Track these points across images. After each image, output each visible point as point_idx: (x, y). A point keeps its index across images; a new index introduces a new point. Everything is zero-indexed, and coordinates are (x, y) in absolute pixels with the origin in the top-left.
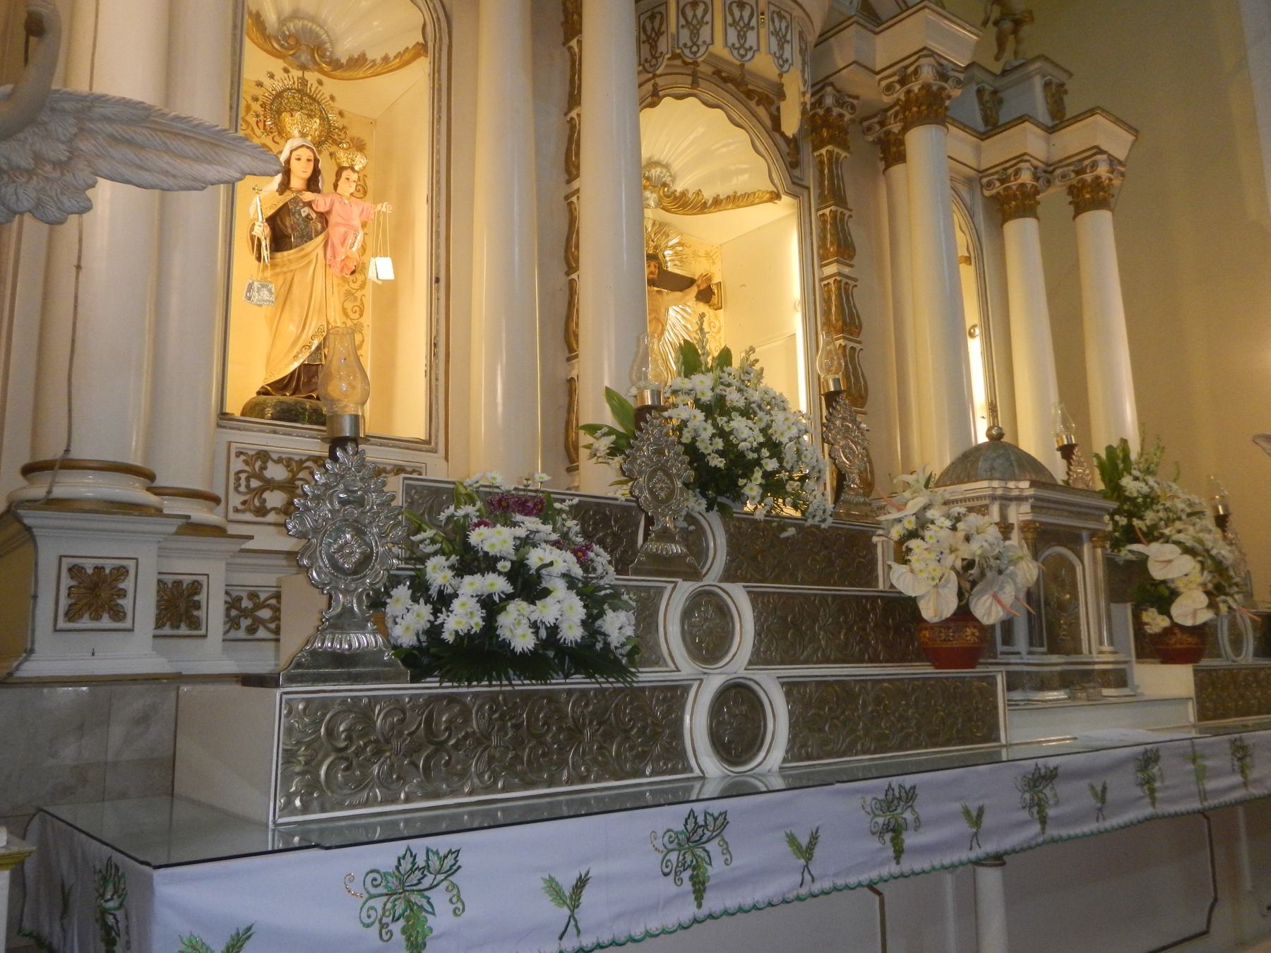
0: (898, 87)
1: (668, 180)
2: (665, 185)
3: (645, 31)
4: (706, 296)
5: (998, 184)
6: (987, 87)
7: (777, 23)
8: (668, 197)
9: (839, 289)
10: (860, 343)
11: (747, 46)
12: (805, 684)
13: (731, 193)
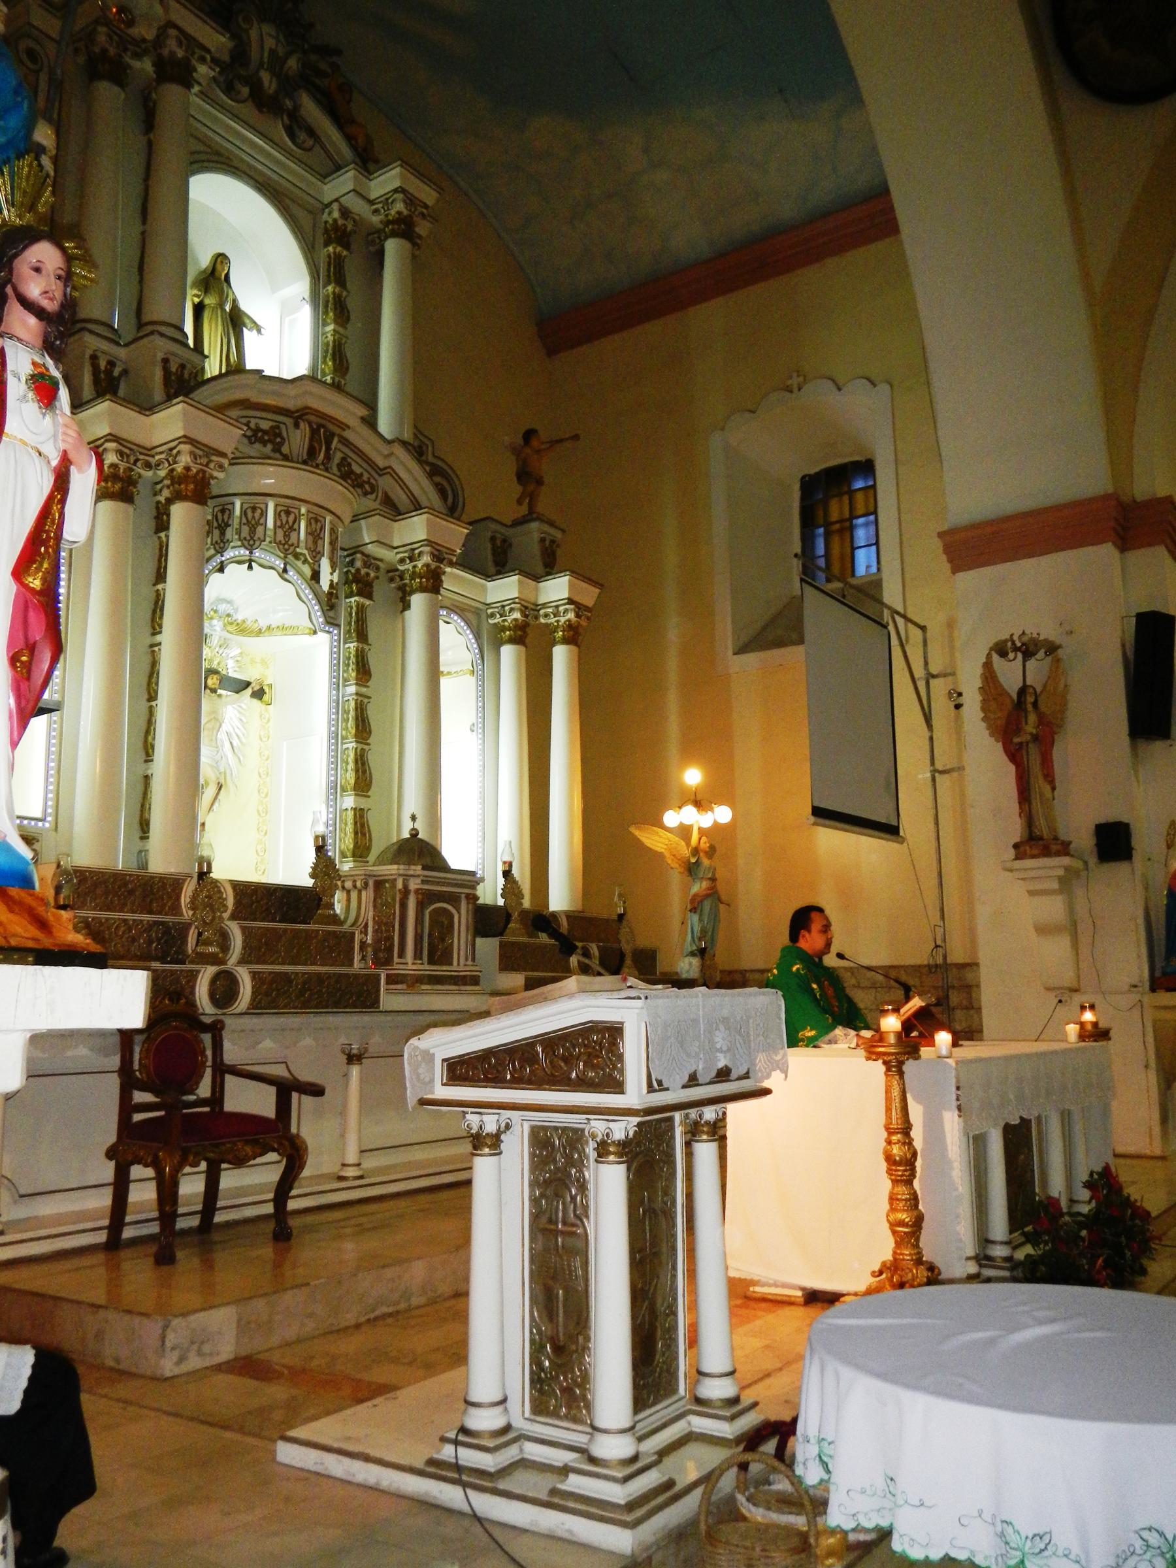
0: (408, 561)
1: (232, 612)
2: (229, 615)
3: (217, 520)
4: (259, 694)
5: (498, 616)
6: (498, 536)
7: (314, 525)
8: (231, 624)
9: (356, 703)
10: (368, 744)
11: (290, 543)
12: (264, 973)
13: (280, 624)
